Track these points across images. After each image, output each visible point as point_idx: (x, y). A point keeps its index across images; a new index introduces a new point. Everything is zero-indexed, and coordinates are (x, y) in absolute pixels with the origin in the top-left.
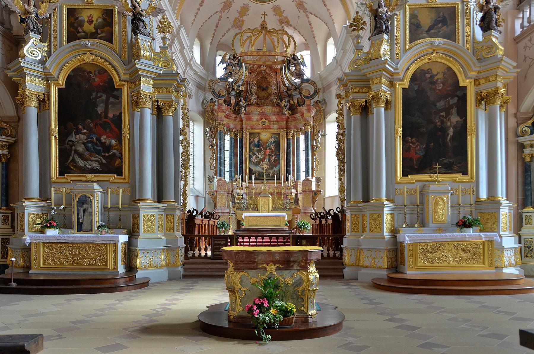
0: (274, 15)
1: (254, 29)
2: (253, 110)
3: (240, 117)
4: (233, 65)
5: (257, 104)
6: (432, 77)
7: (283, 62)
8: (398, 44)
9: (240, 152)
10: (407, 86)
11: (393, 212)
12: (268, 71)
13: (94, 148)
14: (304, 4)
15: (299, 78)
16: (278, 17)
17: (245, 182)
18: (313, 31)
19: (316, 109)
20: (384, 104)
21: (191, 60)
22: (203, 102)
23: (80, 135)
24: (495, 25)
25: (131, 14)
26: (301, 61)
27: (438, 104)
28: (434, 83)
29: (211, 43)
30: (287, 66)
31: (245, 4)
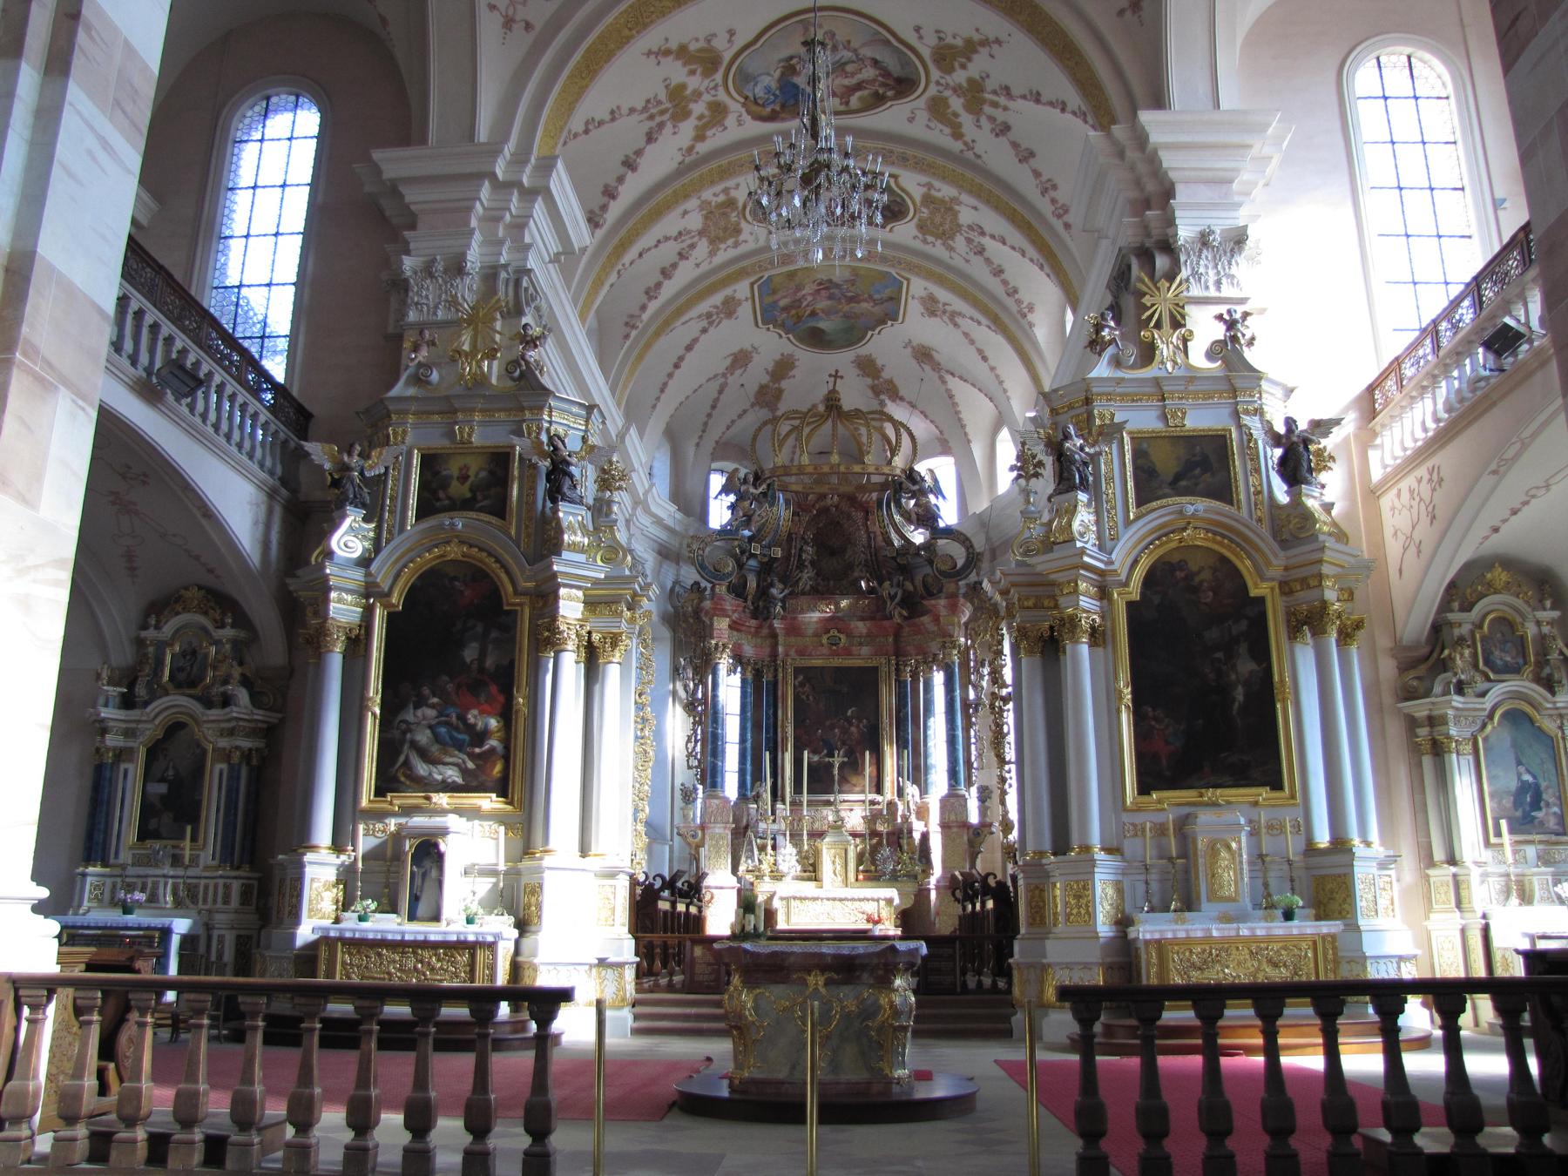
3: (771, 626)
6: (1190, 576)
7: (883, 487)
9: (767, 719)
10: (1136, 596)
11: (1120, 878)
12: (845, 506)
13: (452, 737)
14: (934, 353)
16: (869, 381)
17: (783, 802)
18: (957, 413)
19: (973, 605)
20: (1086, 636)
22: (672, 589)
23: (424, 708)
25: (547, 463)
26: (929, 481)
28: (1195, 590)
29: (698, 445)
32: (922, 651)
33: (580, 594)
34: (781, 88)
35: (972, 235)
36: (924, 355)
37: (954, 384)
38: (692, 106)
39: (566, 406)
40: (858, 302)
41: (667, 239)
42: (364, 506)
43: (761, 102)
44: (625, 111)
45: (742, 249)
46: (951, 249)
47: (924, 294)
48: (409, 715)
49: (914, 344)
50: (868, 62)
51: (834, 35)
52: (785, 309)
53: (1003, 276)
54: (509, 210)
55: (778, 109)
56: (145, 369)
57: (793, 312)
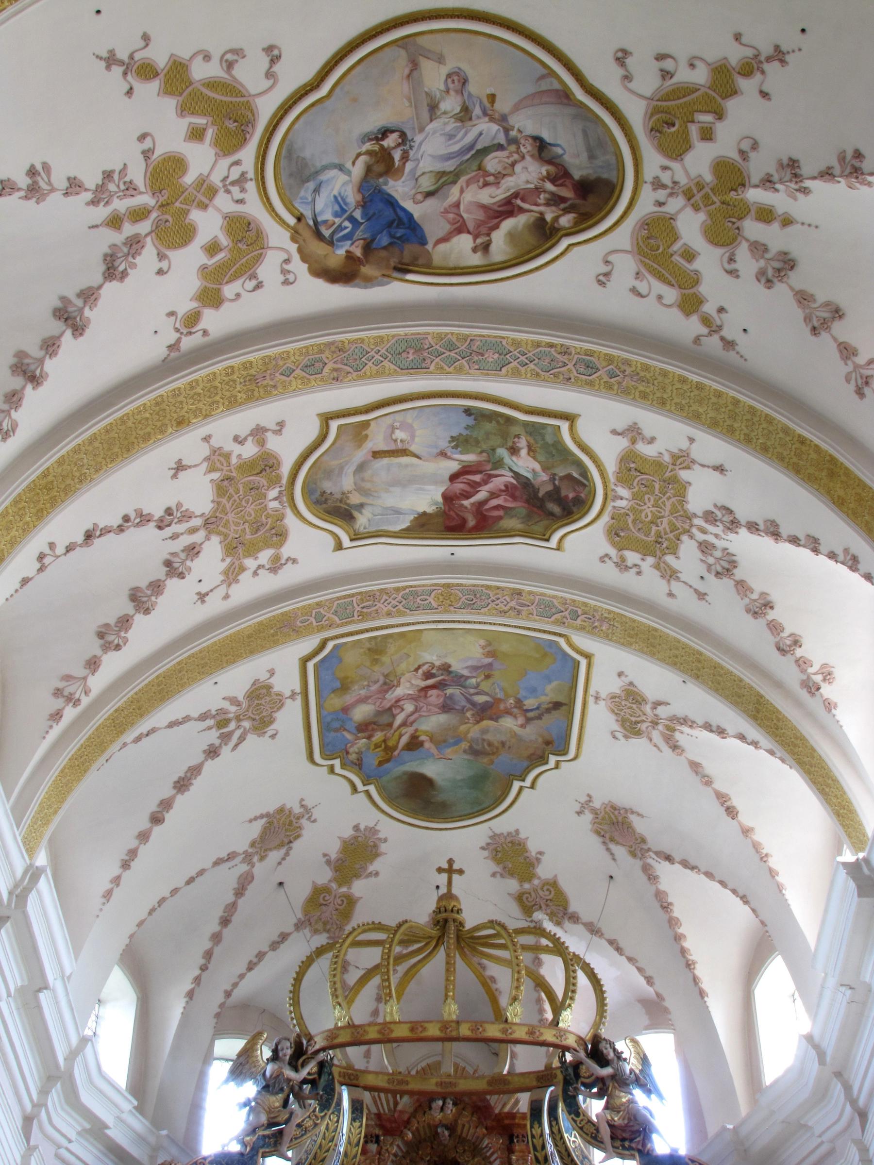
0: (494, 875)
1: (400, 926)
4: (292, 1090)
7: (543, 1078)
12: (469, 1127)
14: (633, 818)
15: (630, 1148)
16: (513, 885)
18: (678, 938)
21: (73, 1055)
30: (565, 1091)
31: (362, 827)
34: (364, 204)
35: (714, 533)
38: (196, 216)
40: (495, 718)
41: (144, 519)
43: (327, 233)
44: (59, 180)
45: (288, 577)
46: (671, 574)
47: (615, 686)
49: (597, 804)
50: (527, 147)
51: (465, 82)
52: (365, 728)
53: (771, 615)
55: (358, 252)
57: (378, 736)
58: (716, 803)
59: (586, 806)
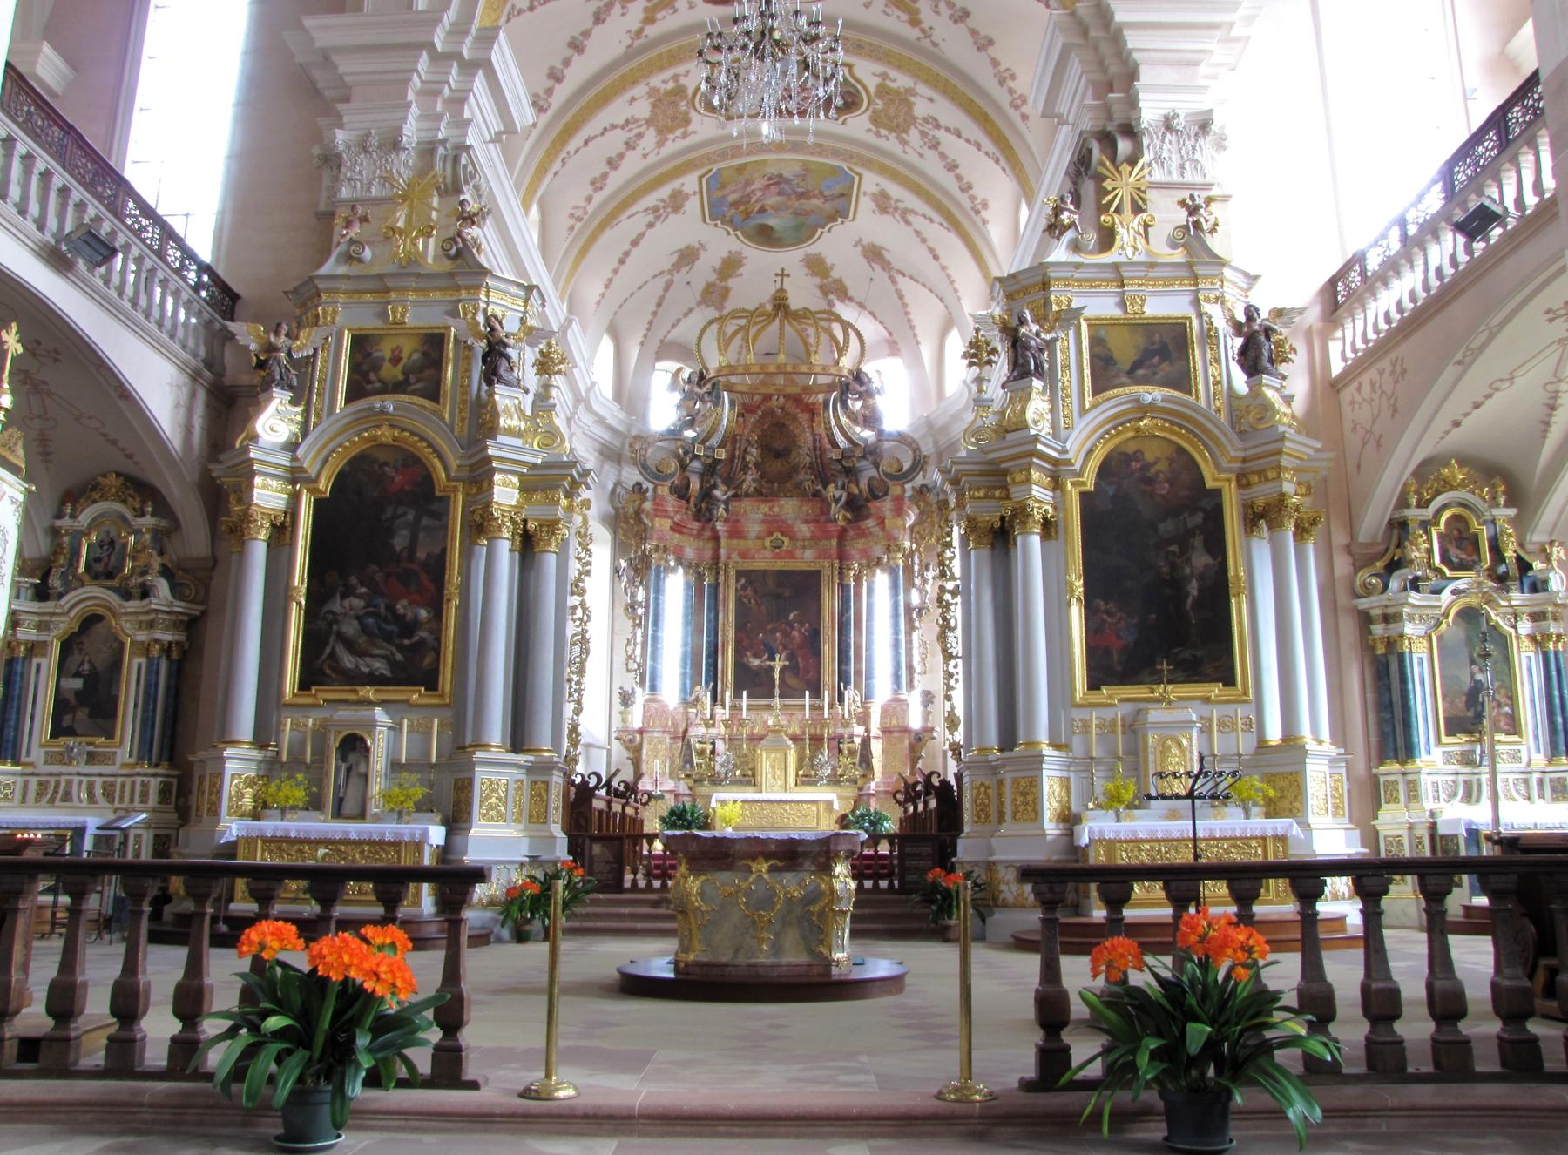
2: (748, 509)
3: (713, 529)
5: (759, 494)
6: (1147, 466)
7: (830, 388)
8: (1067, 396)
9: (709, 621)
10: (1090, 487)
12: (791, 407)
13: (380, 628)
14: (884, 252)
16: (817, 280)
17: (723, 706)
18: (907, 313)
19: (919, 507)
21: (588, 391)
22: (613, 491)
24: (1268, 365)
25: (484, 344)
26: (876, 384)
27: (1161, 527)
28: (1150, 481)
29: (642, 344)
32: (865, 553)
33: (516, 480)
35: (927, 128)
36: (874, 254)
37: (903, 283)
39: (504, 286)
40: (809, 198)
41: (614, 127)
42: (291, 388)
45: (692, 140)
46: (904, 143)
47: (875, 190)
48: (336, 606)
49: (864, 242)
52: (735, 204)
53: (958, 171)
54: (448, 83)
56: (53, 235)
57: (742, 208)
58: (928, 252)
59: (858, 243)
